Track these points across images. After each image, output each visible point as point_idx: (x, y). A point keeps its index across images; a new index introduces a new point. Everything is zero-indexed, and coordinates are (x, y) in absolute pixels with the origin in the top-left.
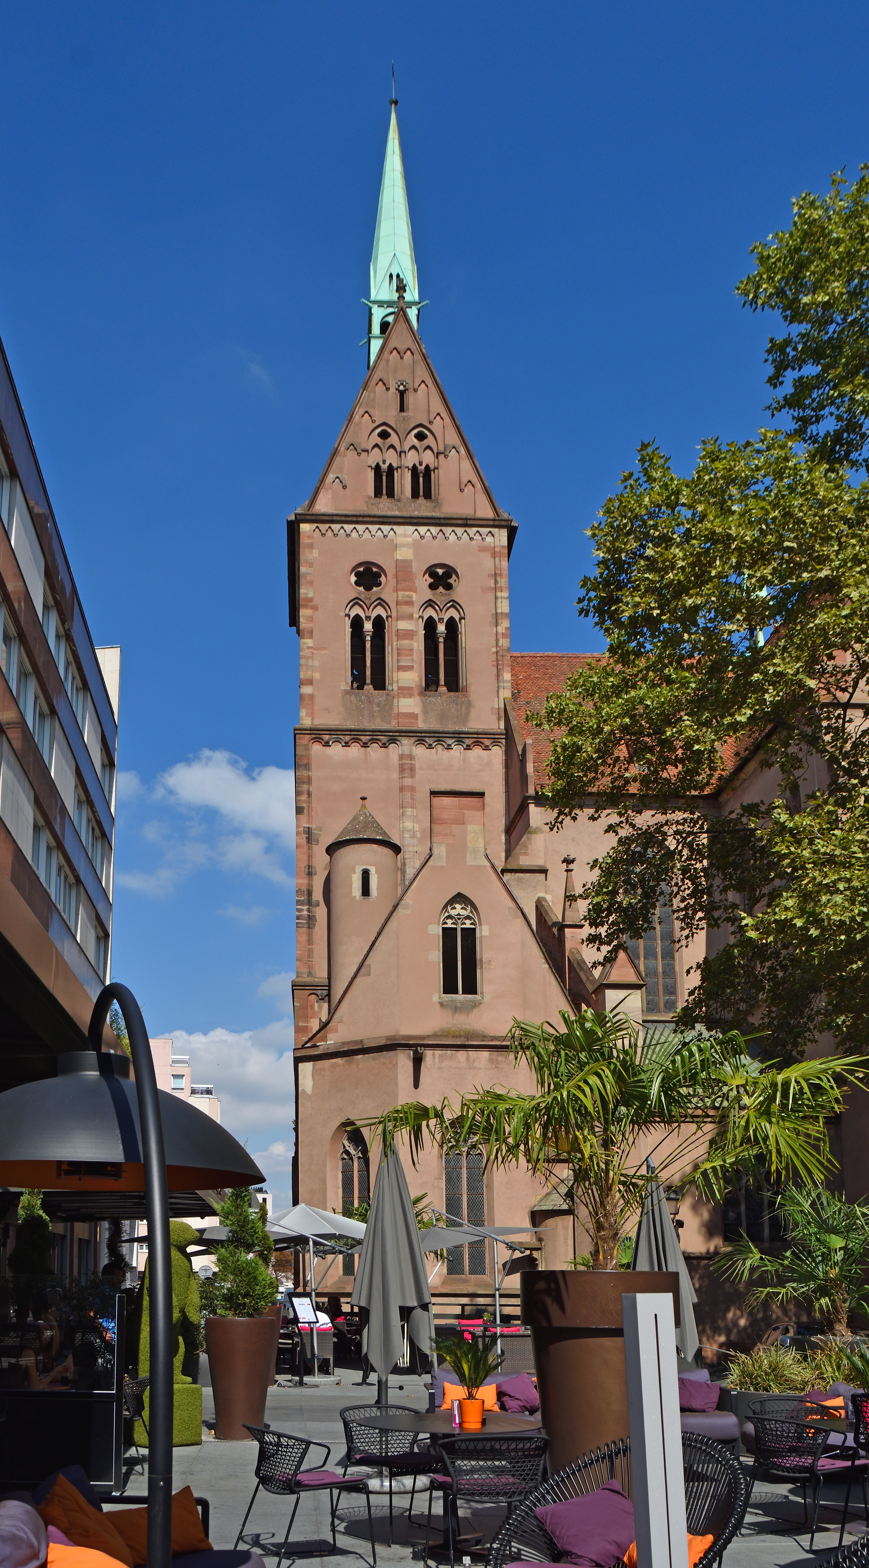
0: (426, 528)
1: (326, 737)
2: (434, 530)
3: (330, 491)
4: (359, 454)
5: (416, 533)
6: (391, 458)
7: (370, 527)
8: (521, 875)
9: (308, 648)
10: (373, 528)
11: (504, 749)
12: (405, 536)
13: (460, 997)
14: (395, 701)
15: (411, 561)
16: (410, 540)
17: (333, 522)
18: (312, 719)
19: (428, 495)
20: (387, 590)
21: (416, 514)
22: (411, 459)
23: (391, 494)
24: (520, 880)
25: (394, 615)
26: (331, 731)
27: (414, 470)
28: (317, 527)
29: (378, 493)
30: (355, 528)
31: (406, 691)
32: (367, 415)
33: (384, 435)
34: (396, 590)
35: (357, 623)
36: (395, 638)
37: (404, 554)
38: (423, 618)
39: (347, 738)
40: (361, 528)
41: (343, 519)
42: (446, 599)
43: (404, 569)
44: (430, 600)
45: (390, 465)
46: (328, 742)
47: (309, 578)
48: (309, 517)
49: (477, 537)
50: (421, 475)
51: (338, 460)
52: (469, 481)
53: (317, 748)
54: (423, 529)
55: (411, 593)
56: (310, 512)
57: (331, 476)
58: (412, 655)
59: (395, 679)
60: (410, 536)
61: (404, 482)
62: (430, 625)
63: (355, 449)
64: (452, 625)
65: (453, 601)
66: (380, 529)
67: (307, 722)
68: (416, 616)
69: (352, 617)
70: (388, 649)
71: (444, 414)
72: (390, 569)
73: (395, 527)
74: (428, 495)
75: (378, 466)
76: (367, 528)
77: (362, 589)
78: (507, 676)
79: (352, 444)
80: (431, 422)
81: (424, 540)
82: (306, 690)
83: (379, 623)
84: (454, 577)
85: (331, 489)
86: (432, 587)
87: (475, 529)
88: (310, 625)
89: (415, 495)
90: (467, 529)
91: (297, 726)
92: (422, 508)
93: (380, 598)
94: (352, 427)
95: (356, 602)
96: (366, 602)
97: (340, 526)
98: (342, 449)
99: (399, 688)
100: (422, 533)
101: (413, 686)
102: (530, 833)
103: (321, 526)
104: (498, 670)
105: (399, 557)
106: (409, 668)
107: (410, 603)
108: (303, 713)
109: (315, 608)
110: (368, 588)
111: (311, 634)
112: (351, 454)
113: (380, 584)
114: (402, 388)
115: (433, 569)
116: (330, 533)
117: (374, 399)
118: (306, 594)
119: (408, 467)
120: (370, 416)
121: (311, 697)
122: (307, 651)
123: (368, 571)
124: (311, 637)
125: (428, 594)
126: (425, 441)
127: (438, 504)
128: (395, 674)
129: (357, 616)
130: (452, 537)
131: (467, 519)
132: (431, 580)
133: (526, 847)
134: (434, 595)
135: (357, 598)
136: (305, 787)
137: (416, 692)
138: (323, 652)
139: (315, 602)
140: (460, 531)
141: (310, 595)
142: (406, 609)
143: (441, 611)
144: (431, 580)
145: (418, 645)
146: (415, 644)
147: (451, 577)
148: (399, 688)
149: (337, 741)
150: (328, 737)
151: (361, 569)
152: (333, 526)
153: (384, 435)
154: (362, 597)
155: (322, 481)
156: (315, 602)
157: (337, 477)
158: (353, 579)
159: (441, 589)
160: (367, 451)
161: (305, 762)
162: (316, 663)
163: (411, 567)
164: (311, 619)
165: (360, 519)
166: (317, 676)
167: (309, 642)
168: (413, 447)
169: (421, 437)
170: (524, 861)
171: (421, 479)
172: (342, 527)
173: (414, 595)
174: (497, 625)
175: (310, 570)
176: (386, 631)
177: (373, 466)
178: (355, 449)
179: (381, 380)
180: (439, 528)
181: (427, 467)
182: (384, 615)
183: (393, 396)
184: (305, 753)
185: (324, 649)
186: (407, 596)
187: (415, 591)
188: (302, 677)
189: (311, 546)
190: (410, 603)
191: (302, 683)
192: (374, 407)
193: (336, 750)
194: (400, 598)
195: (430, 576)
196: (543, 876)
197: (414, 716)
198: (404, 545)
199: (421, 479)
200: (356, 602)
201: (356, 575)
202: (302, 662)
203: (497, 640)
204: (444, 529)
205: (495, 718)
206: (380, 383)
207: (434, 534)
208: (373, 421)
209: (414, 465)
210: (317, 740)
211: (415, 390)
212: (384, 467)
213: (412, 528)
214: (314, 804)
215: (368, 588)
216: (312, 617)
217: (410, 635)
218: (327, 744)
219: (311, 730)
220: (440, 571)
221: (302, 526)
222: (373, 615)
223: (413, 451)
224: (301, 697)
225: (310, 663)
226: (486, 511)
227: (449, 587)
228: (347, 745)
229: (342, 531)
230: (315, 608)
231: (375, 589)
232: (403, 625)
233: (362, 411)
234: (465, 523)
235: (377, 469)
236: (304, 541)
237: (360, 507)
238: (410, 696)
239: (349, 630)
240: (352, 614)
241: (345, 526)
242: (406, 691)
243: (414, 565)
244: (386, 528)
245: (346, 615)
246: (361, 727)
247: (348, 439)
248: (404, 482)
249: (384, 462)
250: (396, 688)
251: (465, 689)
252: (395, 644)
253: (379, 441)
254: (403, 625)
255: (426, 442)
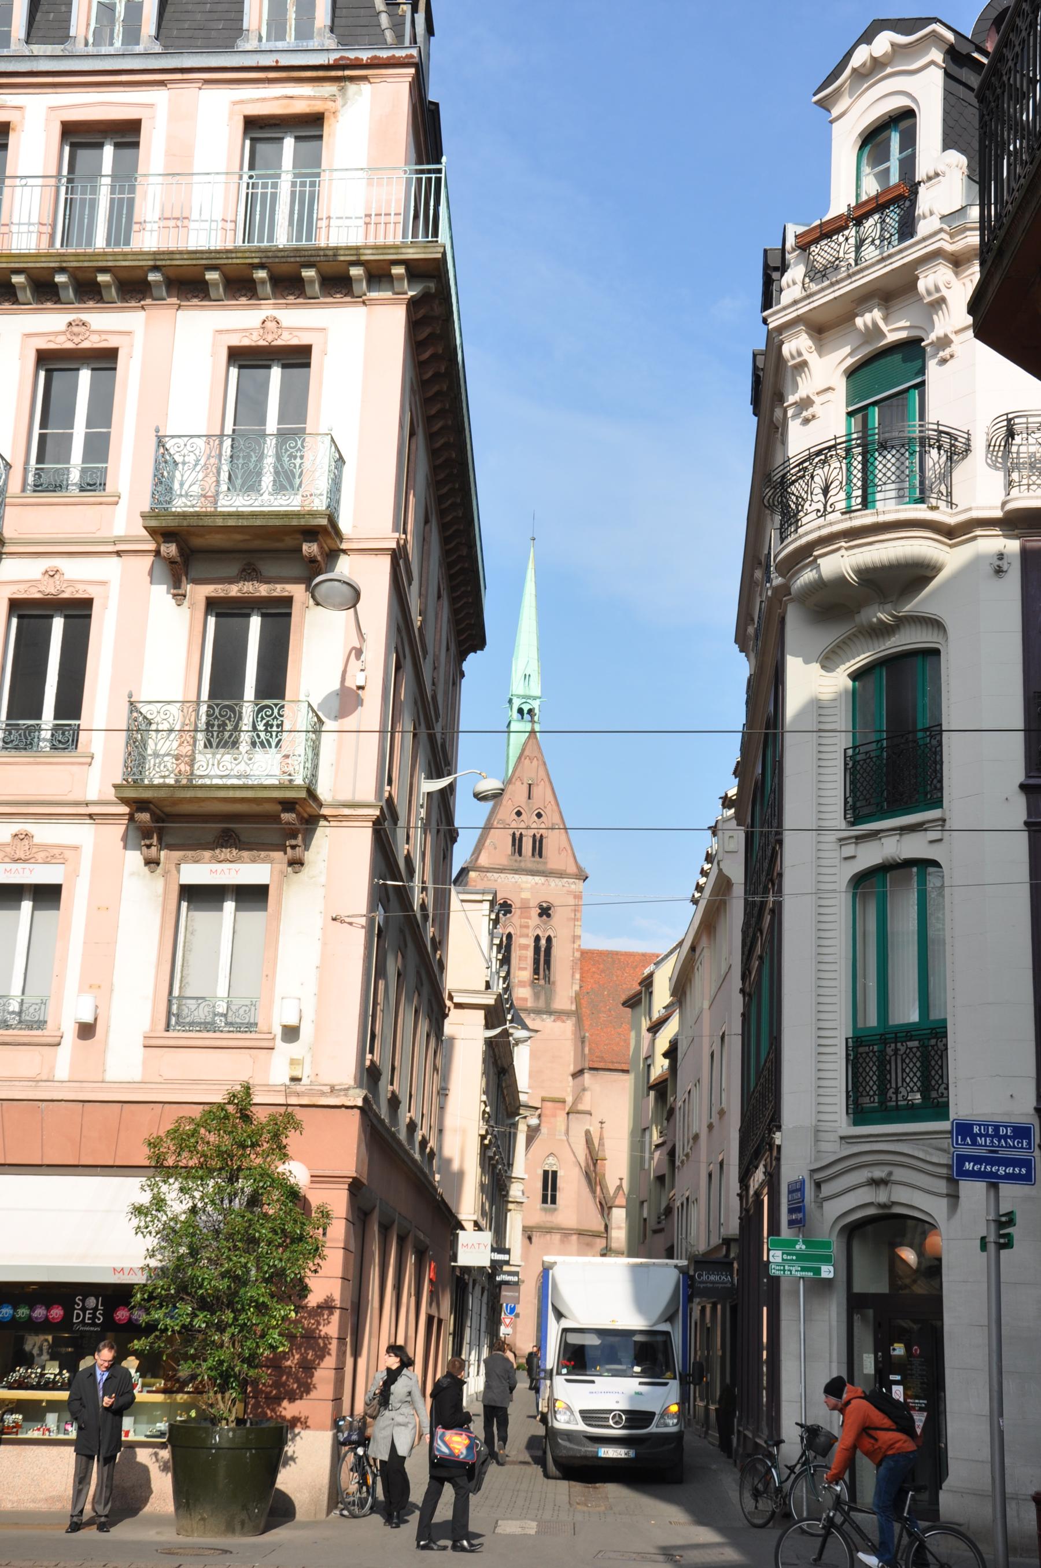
12: (527, 882)
13: (549, 1205)
15: (529, 899)
23: (520, 854)
31: (522, 984)
33: (519, 814)
34: (520, 918)
37: (525, 895)
49: (567, 885)
54: (537, 879)
61: (527, 845)
62: (537, 939)
64: (549, 939)
71: (553, 802)
78: (578, 976)
80: (545, 807)
86: (540, 915)
87: (565, 880)
89: (533, 855)
99: (519, 981)
104: (573, 973)
106: (525, 969)
107: (527, 927)
114: (530, 782)
127: (545, 863)
130: (553, 884)
132: (540, 911)
134: (541, 921)
137: (528, 984)
140: (557, 880)
142: (525, 931)
144: (540, 911)
145: (530, 953)
148: (519, 981)
153: (519, 814)
159: (545, 917)
169: (539, 815)
174: (574, 942)
181: (541, 836)
183: (525, 787)
190: (527, 927)
197: (526, 1000)
203: (574, 953)
205: (569, 1002)
211: (538, 785)
213: (530, 878)
217: (525, 947)
220: (545, 905)
222: (507, 932)
226: (572, 869)
227: (549, 916)
232: (523, 941)
234: (560, 875)
238: (524, 986)
242: (522, 984)
248: (527, 845)
251: (554, 983)
253: (516, 817)
254: (523, 941)
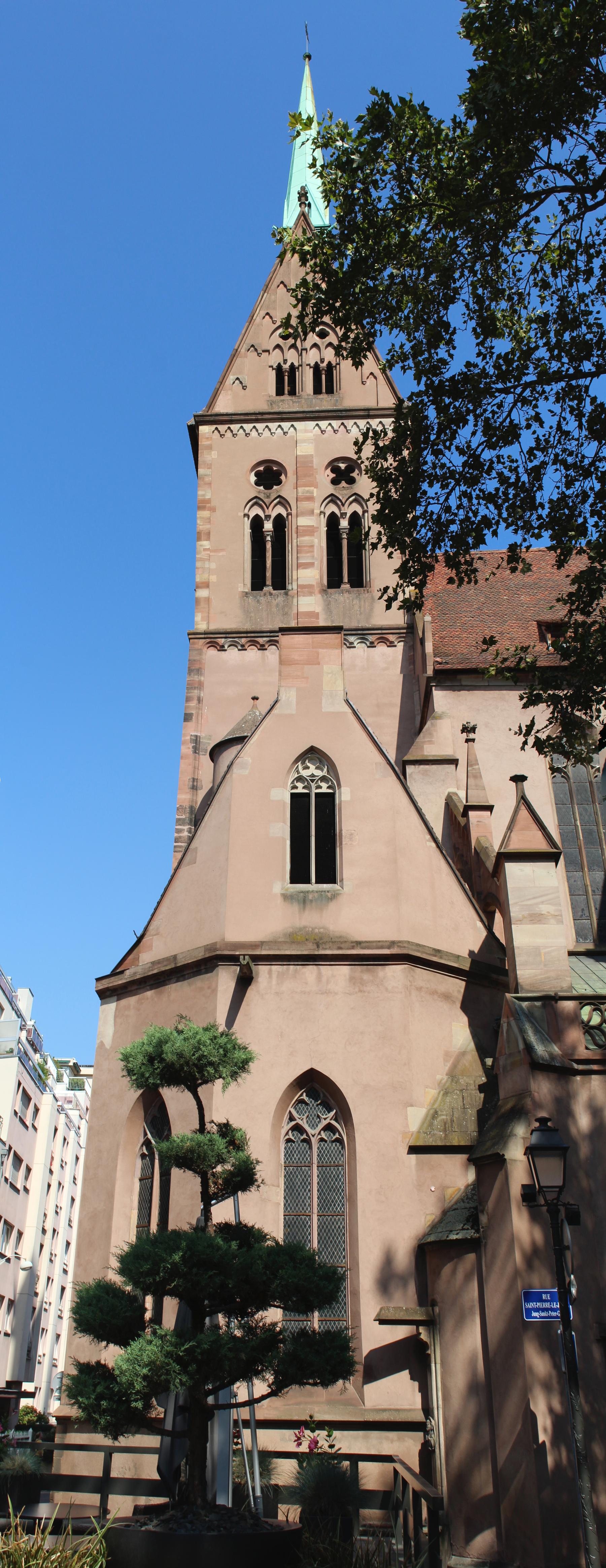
0: (327, 422)
1: (221, 641)
2: (336, 423)
3: (230, 392)
4: (259, 355)
5: (317, 428)
6: (292, 357)
7: (270, 425)
8: (427, 767)
9: (205, 550)
10: (273, 426)
11: (400, 646)
12: (306, 431)
14: (295, 600)
15: (312, 456)
16: (310, 435)
17: (232, 422)
18: (208, 623)
19: (330, 390)
20: (287, 489)
21: (317, 408)
22: (312, 357)
23: (292, 392)
24: (425, 773)
25: (294, 512)
26: (226, 634)
27: (316, 368)
28: (216, 429)
29: (280, 392)
30: (254, 427)
32: (267, 317)
35: (257, 524)
36: (294, 535)
37: (305, 449)
38: (325, 514)
39: (243, 641)
40: (260, 426)
41: (242, 417)
42: (348, 493)
43: (304, 465)
44: (332, 495)
45: (292, 364)
46: (223, 646)
47: (207, 479)
48: (208, 419)
50: (324, 372)
51: (238, 361)
52: (372, 374)
53: (212, 652)
54: (324, 424)
55: (312, 488)
56: (209, 413)
57: (231, 378)
58: (313, 552)
59: (295, 577)
60: (311, 432)
61: (307, 379)
63: (256, 350)
65: (355, 494)
66: (280, 426)
67: (202, 626)
68: (317, 511)
69: (251, 517)
70: (289, 547)
72: (290, 468)
73: (295, 424)
74: (330, 390)
75: (279, 366)
76: (267, 427)
77: (262, 488)
79: (253, 346)
81: (326, 435)
82: (202, 593)
83: (280, 523)
84: (357, 471)
85: (231, 389)
86: (335, 482)
88: (208, 526)
89: (317, 390)
90: (369, 420)
91: (192, 631)
92: (325, 402)
93: (279, 496)
94: (252, 329)
95: (256, 501)
96: (266, 500)
97: (239, 426)
98: (243, 351)
100: (323, 428)
101: (314, 583)
102: (435, 718)
103: (220, 427)
105: (299, 453)
106: (310, 565)
107: (310, 499)
108: (198, 617)
109: (213, 510)
110: (268, 487)
111: (208, 535)
112: (252, 354)
113: (279, 482)
115: (336, 464)
116: (229, 434)
117: (275, 301)
118: (203, 495)
119: (309, 365)
120: (271, 317)
121: (208, 600)
122: (203, 553)
123: (268, 470)
124: (208, 539)
125: (330, 489)
126: (327, 338)
128: (295, 573)
129: (257, 516)
131: (368, 410)
132: (333, 475)
133: (431, 734)
135: (256, 497)
136: (196, 693)
138: (221, 554)
139: (213, 504)
141: (208, 496)
142: (305, 505)
143: (343, 505)
144: (333, 475)
146: (316, 541)
147: (353, 471)
149: (233, 645)
150: (223, 640)
151: (261, 468)
152: (232, 426)
154: (262, 496)
155: (221, 382)
156: (213, 504)
157: (238, 379)
158: (253, 478)
159: (343, 484)
160: (268, 351)
161: (197, 666)
162: (213, 566)
163: (312, 462)
164: (209, 521)
165: (260, 417)
166: (213, 579)
167: (206, 544)
168: (315, 345)
170: (430, 750)
171: (324, 377)
172: (242, 427)
173: (315, 490)
175: (208, 472)
176: (286, 530)
177: (275, 367)
178: (256, 350)
179: (282, 282)
180: (340, 422)
182: (284, 514)
184: (197, 658)
185: (222, 550)
186: (308, 492)
187: (316, 487)
188: (198, 579)
189: (210, 448)
190: (310, 499)
191: (198, 586)
192: (275, 309)
193: (232, 655)
194: (300, 494)
195: (332, 471)
196: (453, 767)
198: (304, 441)
199: (324, 377)
200: (256, 501)
201: (256, 475)
202: (198, 564)
204: (345, 422)
206: (282, 286)
207: (336, 428)
208: (274, 322)
209: (316, 363)
210: (213, 644)
212: (286, 367)
213: (313, 423)
214: (205, 710)
215: (268, 487)
216: (209, 518)
217: (311, 531)
218: (222, 649)
219: (205, 633)
220: (343, 466)
221: (201, 428)
223: (314, 350)
224: (197, 601)
225: (207, 565)
228: (243, 648)
229: (241, 431)
230: (213, 510)
231: (275, 487)
233: (263, 313)
235: (279, 370)
236: (202, 442)
237: (262, 406)
239: (248, 531)
240: (252, 515)
241: (245, 426)
242: (307, 589)
243: (315, 461)
244: (286, 425)
245: (245, 515)
246: (258, 629)
247: (249, 341)
249: (285, 361)
250: (295, 587)
252: (295, 541)
253: (281, 342)
254: (303, 521)
255: (327, 340)
